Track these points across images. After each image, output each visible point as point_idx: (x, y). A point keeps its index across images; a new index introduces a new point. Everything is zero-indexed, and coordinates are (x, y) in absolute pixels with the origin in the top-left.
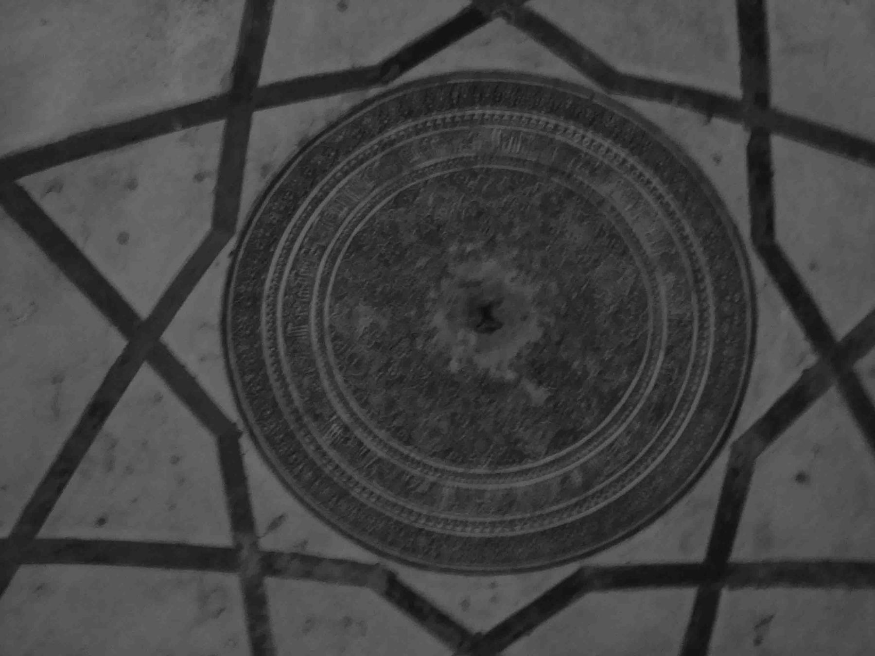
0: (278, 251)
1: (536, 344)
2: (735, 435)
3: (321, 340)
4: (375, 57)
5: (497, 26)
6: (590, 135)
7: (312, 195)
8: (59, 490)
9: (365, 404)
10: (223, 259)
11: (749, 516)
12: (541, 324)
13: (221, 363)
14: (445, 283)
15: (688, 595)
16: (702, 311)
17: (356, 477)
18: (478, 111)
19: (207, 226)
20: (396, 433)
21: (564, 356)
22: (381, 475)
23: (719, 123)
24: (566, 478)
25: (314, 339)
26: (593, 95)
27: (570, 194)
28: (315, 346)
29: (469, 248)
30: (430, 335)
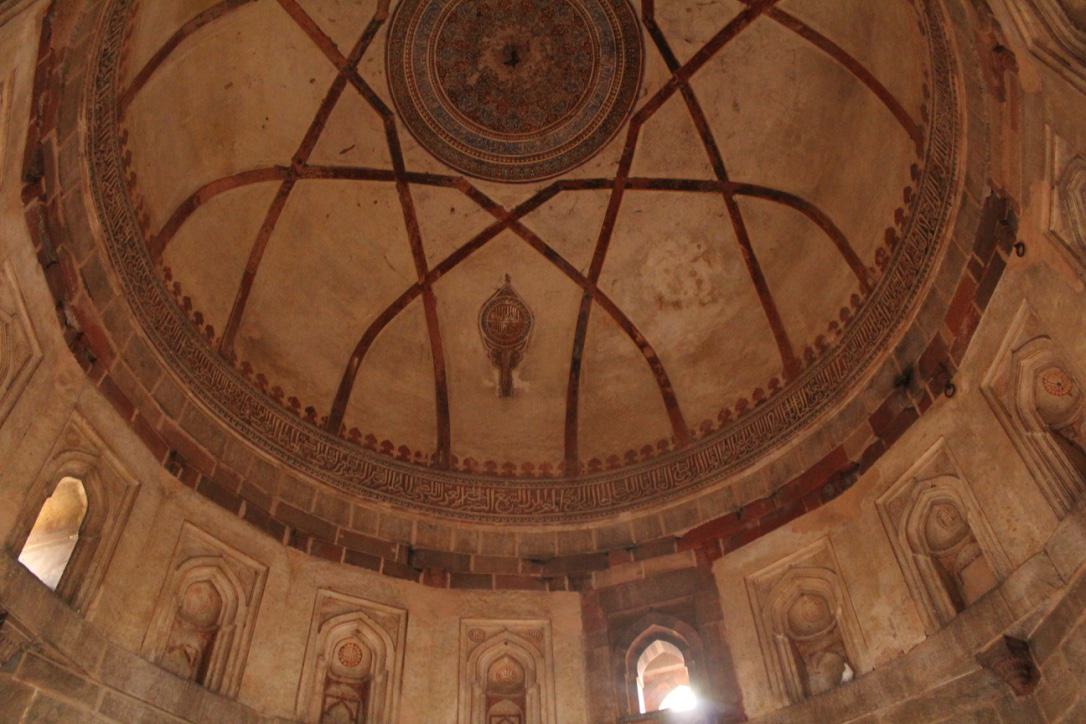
1: (497, 78)
2: (467, 178)
5: (668, 75)
6: (609, 110)
11: (430, 189)
14: (529, 34)
15: (390, 167)
18: (624, 60)
20: (454, 14)
21: (493, 92)
22: (433, 9)
23: (616, 168)
24: (435, 100)
26: (630, 113)
27: (578, 97)
29: (548, 47)
30: (502, 28)
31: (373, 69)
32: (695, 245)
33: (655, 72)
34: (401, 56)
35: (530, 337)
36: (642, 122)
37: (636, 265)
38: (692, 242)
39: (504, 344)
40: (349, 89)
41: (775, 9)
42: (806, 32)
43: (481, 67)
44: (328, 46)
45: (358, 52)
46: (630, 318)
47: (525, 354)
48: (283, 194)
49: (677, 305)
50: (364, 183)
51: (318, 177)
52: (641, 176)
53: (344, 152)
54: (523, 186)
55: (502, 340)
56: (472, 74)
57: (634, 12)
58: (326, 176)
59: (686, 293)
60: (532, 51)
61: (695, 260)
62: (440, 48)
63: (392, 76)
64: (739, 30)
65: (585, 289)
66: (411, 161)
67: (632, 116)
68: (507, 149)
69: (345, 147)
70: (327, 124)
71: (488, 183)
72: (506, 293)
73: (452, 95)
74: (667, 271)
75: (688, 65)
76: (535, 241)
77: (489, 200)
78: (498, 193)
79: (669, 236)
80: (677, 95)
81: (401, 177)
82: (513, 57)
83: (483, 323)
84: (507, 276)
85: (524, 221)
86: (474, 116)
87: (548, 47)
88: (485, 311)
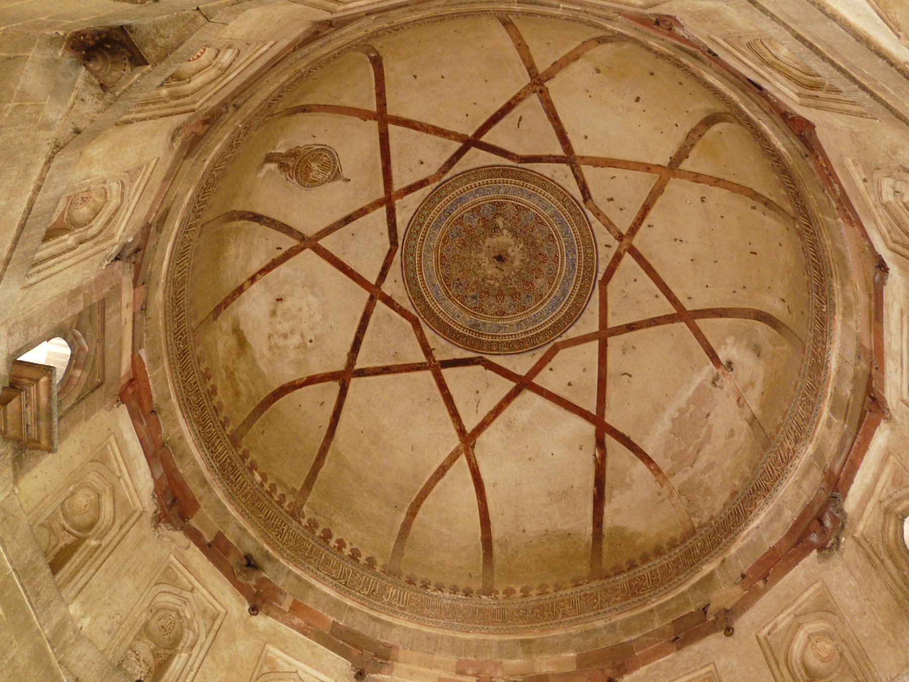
0: (547, 326)
1: (491, 236)
2: (437, 183)
3: (555, 287)
4: (480, 368)
5: (439, 357)
6: (431, 306)
7: (526, 336)
8: (659, 318)
9: (556, 256)
10: (564, 338)
11: (447, 156)
12: (484, 242)
13: (588, 307)
14: (507, 275)
16: (427, 230)
17: (574, 238)
19: (561, 352)
20: (554, 241)
21: (483, 229)
22: (567, 233)
23: (389, 295)
25: (557, 289)
28: (558, 286)
29: (492, 282)
31: (561, 174)
32: (313, 338)
33: (444, 349)
34: (552, 194)
35: (293, 183)
36: (413, 326)
37: (311, 285)
38: (316, 337)
39: (300, 161)
40: (558, 150)
41: (461, 453)
42: (442, 471)
43: (505, 232)
44: (597, 162)
45: (578, 174)
46: (275, 271)
47: (283, 176)
48: (531, 68)
49: (273, 313)
50: (488, 117)
51: (519, 94)
52: (375, 310)
53: (520, 119)
54: (409, 220)
55: (303, 161)
56: (504, 223)
57: (490, 354)
58: (514, 98)
59: (280, 323)
60: (495, 269)
61: (302, 336)
62: (537, 217)
63: (543, 180)
64: (454, 421)
65: (310, 239)
66: (477, 154)
67: (420, 320)
68: (440, 220)
69: (522, 122)
70: (549, 123)
71: (425, 197)
72: (337, 175)
73: (503, 204)
74: (300, 310)
75: (441, 375)
76: (363, 212)
77: (412, 192)
78: (414, 200)
79: (325, 318)
80: (422, 358)
81: (470, 143)
82: (500, 258)
83: (323, 149)
84: (349, 180)
85: (383, 210)
86: (477, 210)
87: (492, 282)
88: (332, 153)
